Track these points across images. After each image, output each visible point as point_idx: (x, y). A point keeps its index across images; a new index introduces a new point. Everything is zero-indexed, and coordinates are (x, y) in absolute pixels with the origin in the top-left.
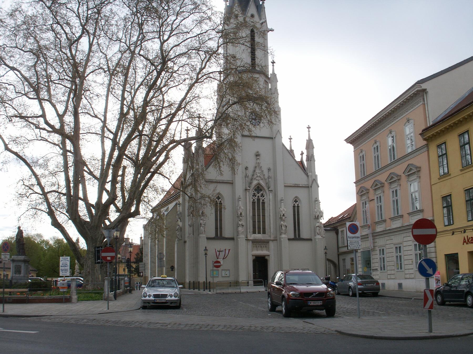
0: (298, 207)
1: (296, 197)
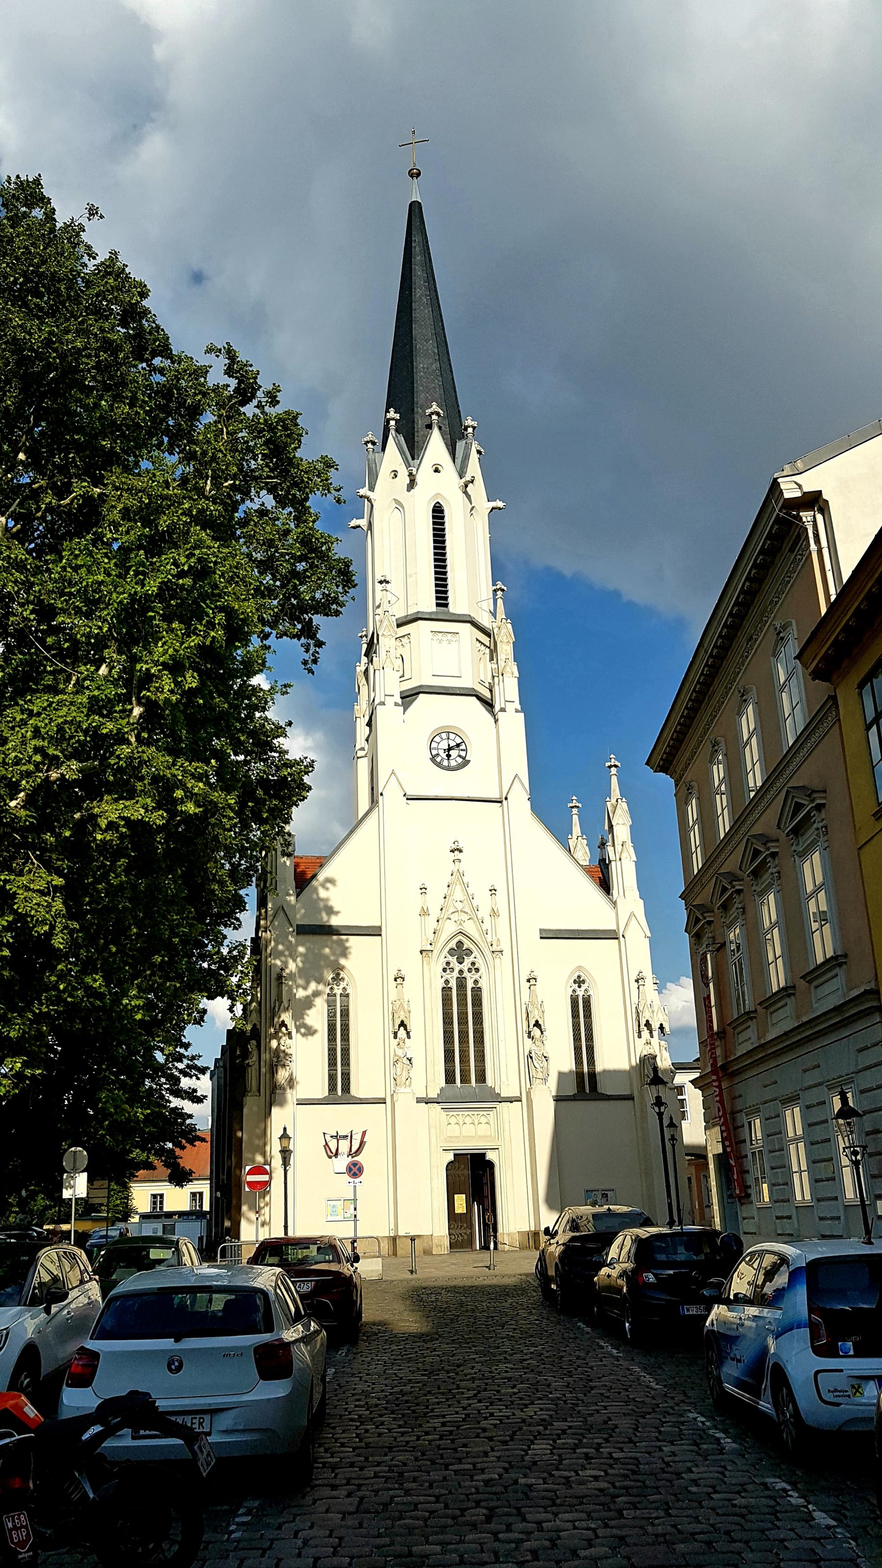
1: (579, 968)
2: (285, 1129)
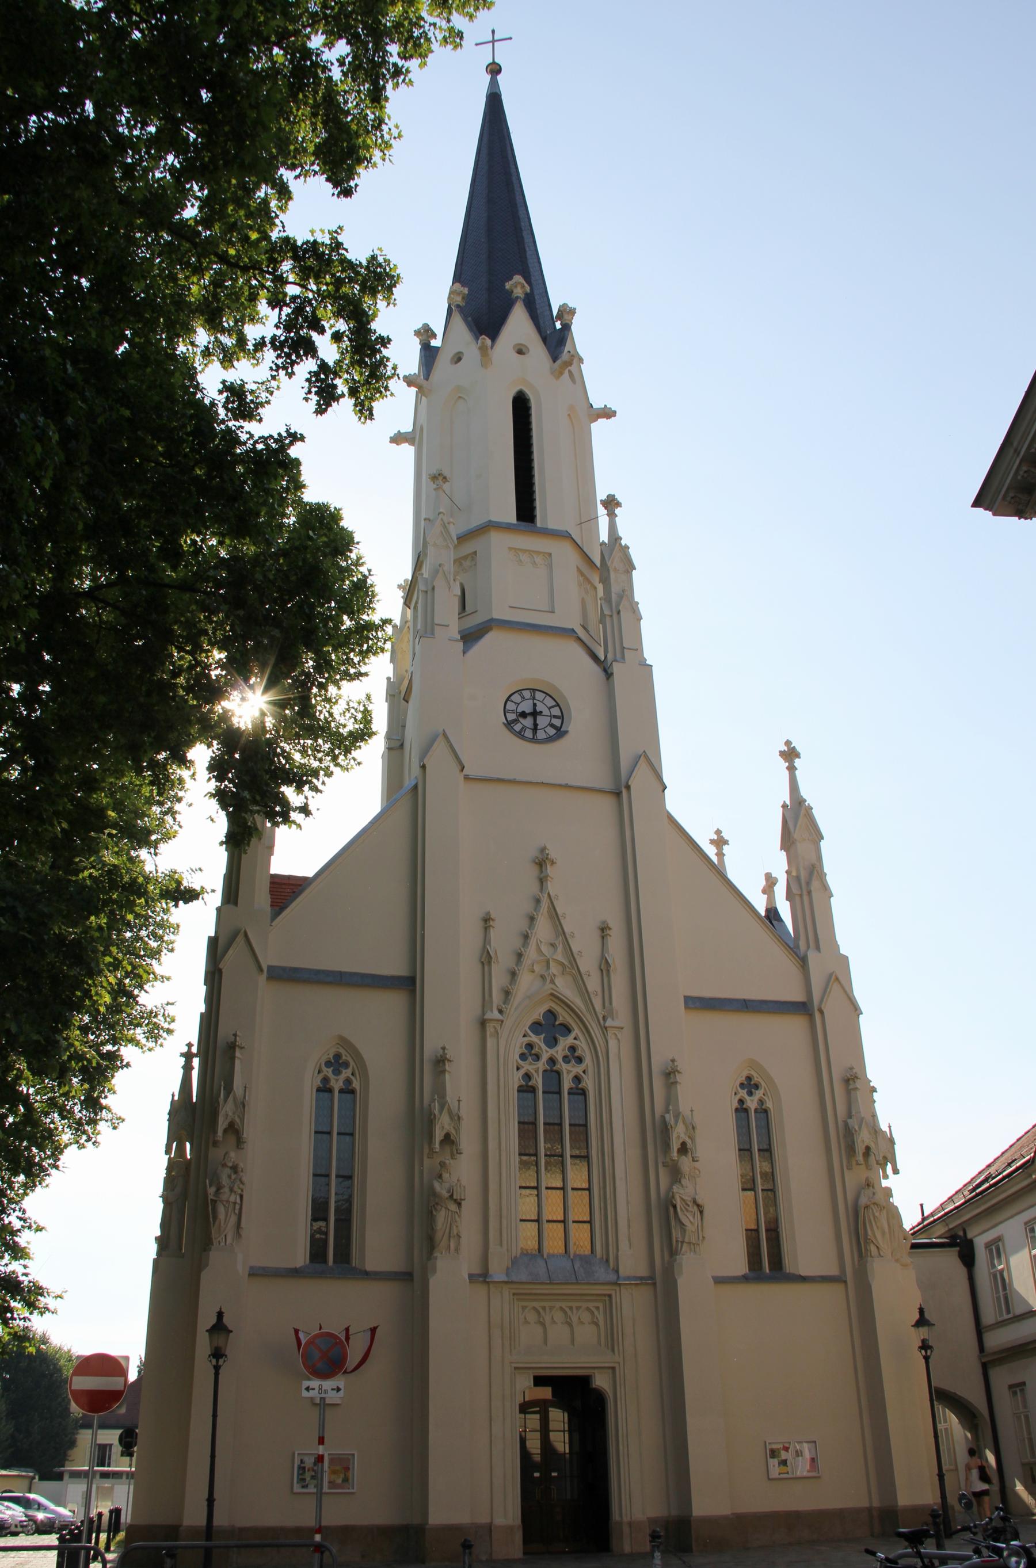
0: (763, 1112)
2: (220, 1315)
